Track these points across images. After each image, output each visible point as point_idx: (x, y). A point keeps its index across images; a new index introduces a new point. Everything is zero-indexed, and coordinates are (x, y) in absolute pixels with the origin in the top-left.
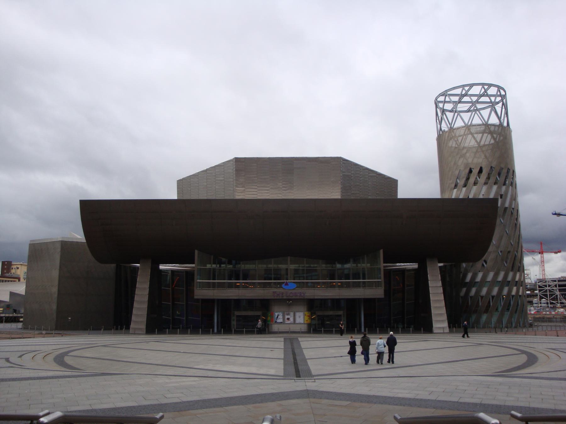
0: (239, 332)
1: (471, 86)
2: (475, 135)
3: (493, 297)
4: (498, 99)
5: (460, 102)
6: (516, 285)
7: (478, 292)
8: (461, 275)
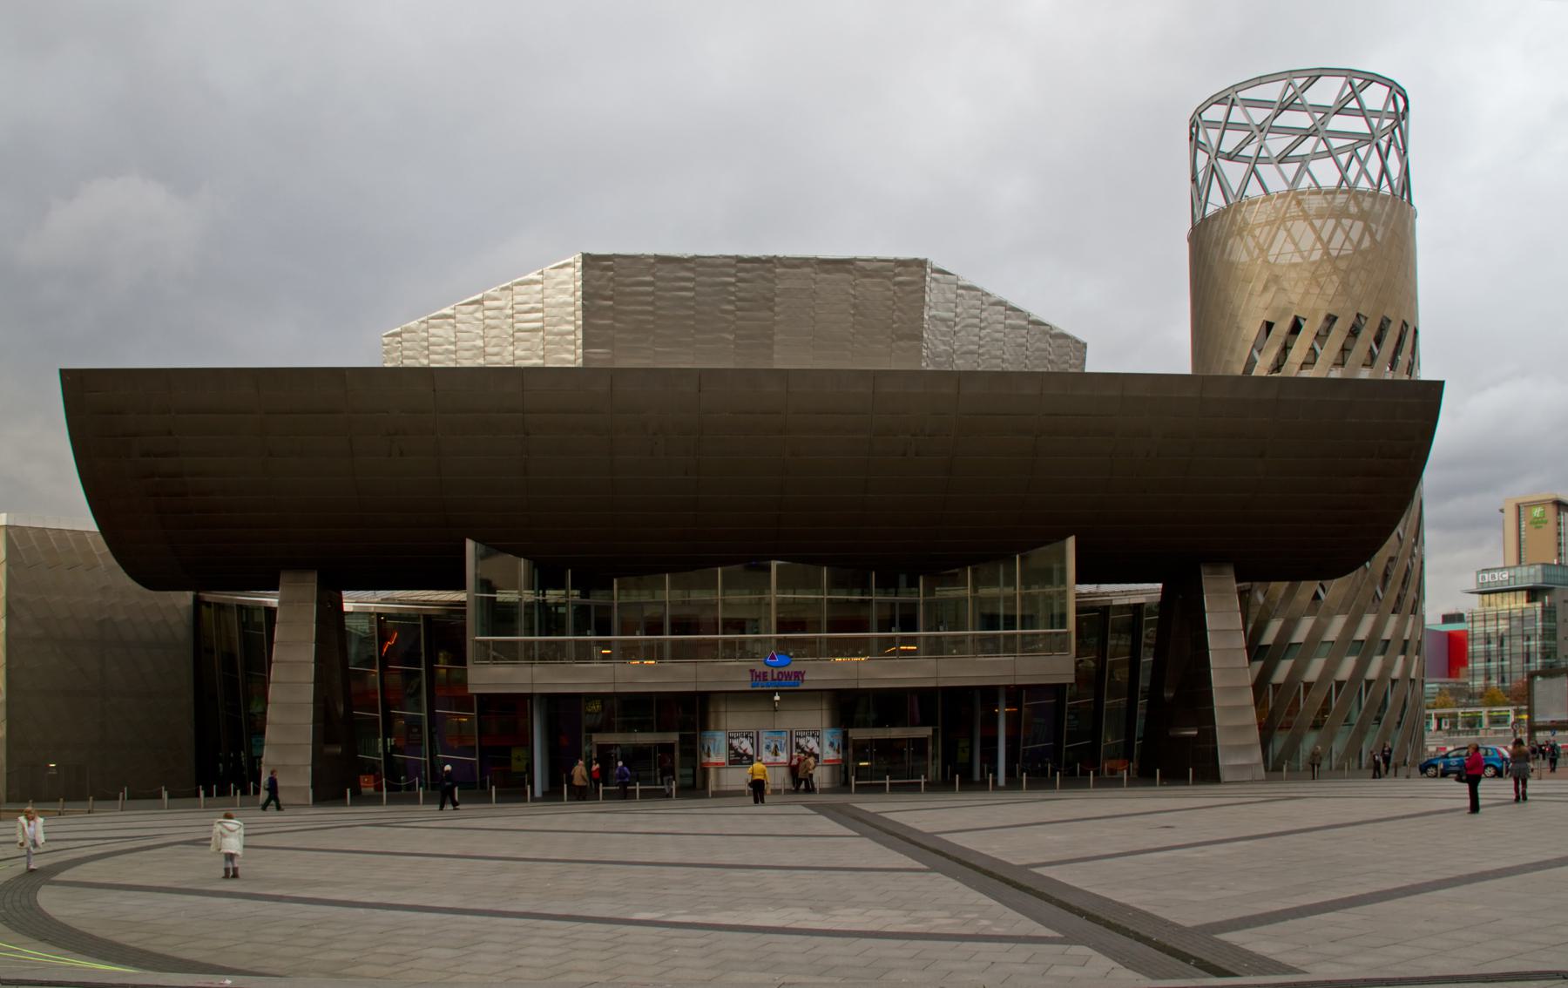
1: (1314, 76)
3: (1339, 684)
6: (1404, 652)
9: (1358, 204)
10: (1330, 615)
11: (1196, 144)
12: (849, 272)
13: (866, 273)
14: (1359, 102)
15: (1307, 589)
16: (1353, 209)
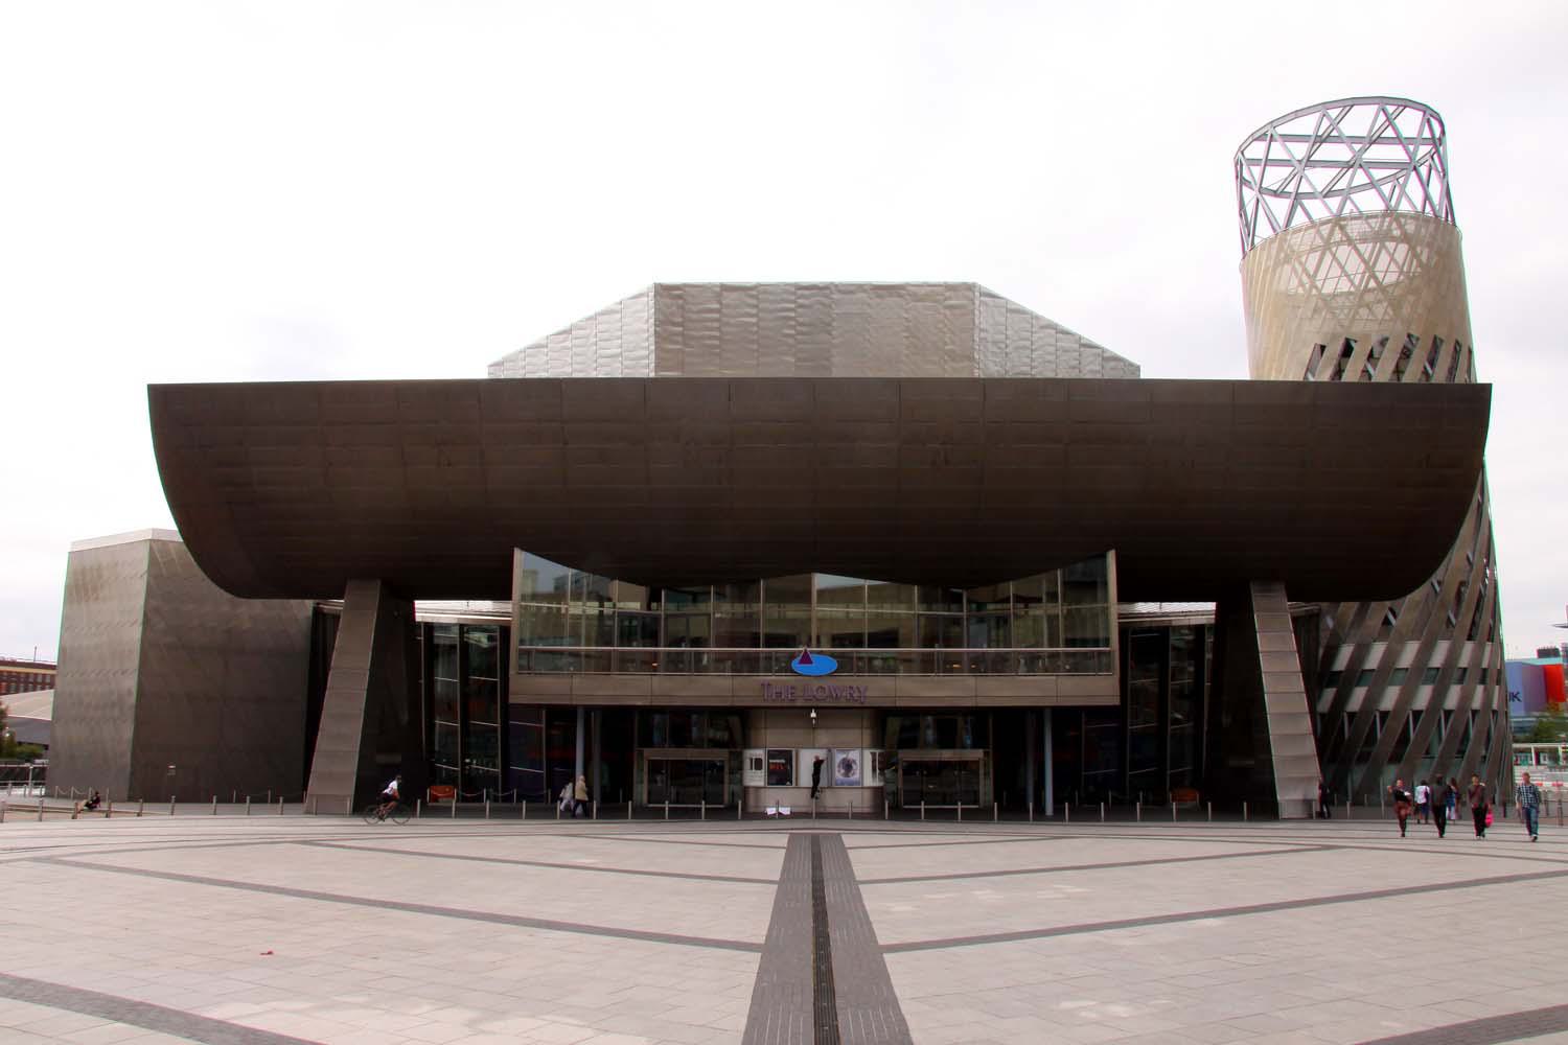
0: (648, 813)
2: (1361, 247)
3: (1417, 714)
4: (1424, 150)
5: (1309, 162)
6: (1483, 681)
7: (1371, 700)
8: (1321, 651)
9: (1400, 226)
10: (1402, 640)
11: (1242, 182)
12: (900, 296)
13: (916, 298)
14: (1395, 129)
15: (1378, 610)
16: (1397, 233)
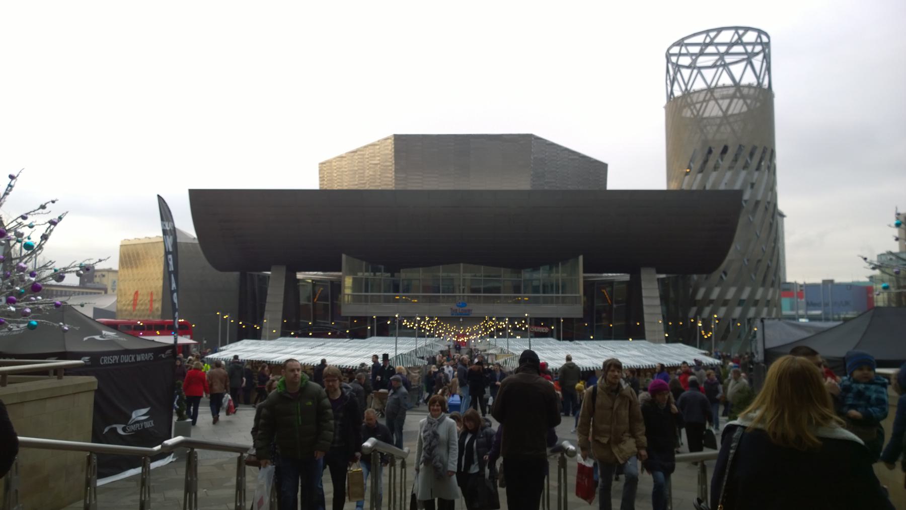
1: (719, 30)
2: (720, 102)
5: (701, 53)
8: (691, 291)
